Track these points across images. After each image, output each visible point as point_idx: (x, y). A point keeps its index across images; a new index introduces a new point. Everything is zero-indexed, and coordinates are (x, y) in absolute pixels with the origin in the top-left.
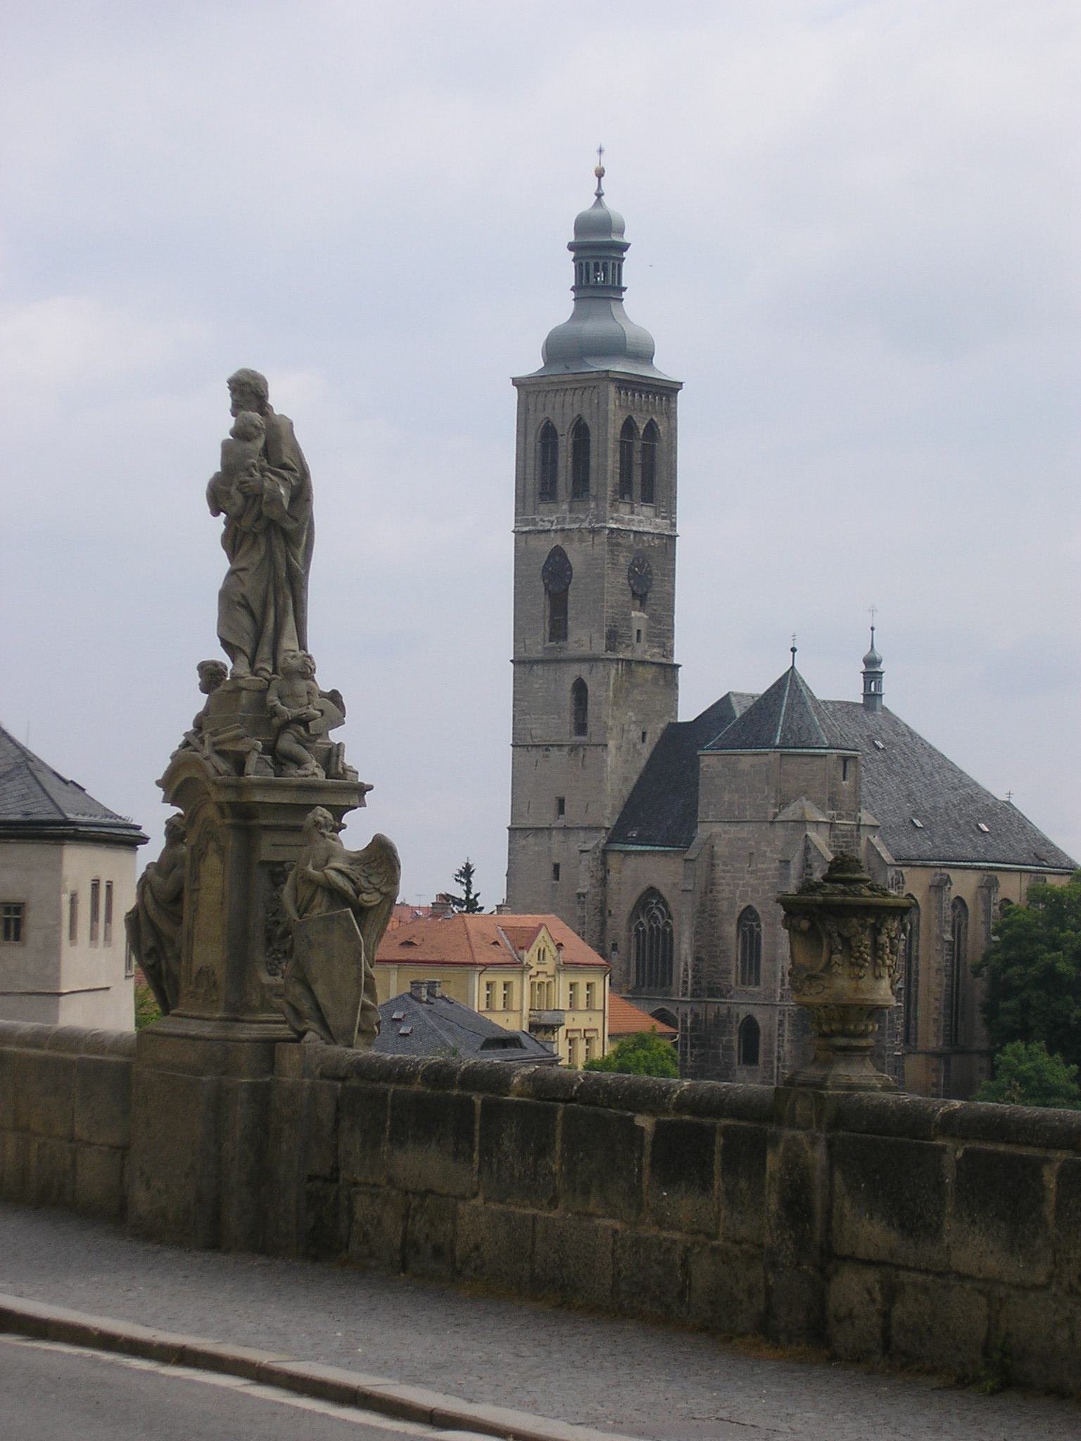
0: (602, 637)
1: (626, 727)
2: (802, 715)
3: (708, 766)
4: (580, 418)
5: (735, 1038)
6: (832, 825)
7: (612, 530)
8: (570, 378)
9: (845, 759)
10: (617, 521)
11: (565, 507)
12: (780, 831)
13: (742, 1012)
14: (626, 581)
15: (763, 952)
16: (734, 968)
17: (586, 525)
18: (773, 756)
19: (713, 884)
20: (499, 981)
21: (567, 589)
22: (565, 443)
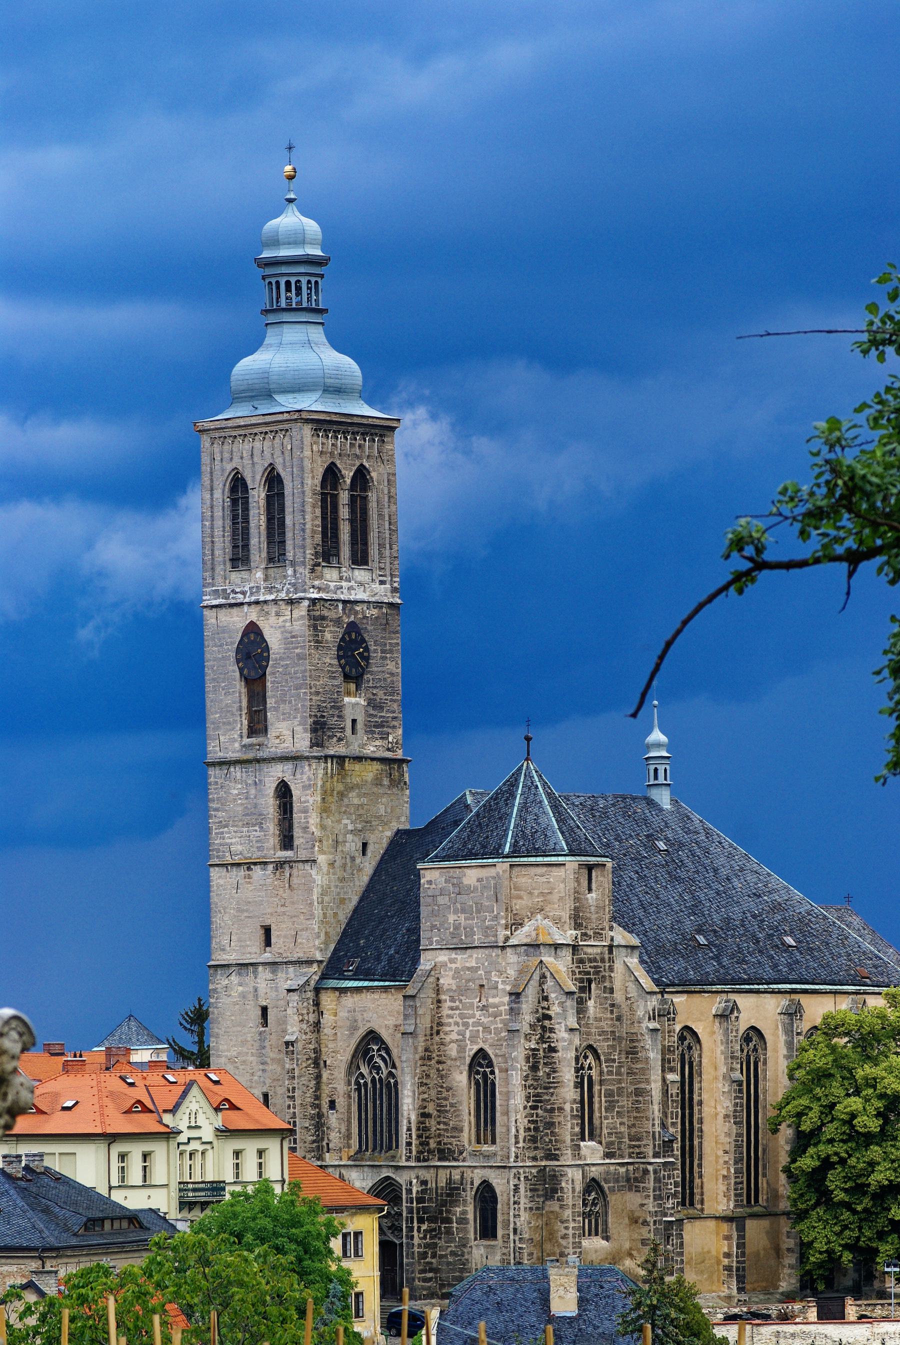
0: (305, 730)
1: (340, 839)
3: (430, 882)
4: (272, 467)
5: (470, 1209)
6: (575, 948)
7: (314, 601)
8: (261, 420)
9: (590, 868)
10: (320, 589)
11: (259, 575)
12: (511, 956)
13: (478, 1177)
14: (335, 662)
15: (498, 1103)
16: (466, 1124)
17: (283, 595)
18: (502, 866)
19: (440, 1024)
20: (136, 1150)
21: (265, 673)
22: (258, 496)
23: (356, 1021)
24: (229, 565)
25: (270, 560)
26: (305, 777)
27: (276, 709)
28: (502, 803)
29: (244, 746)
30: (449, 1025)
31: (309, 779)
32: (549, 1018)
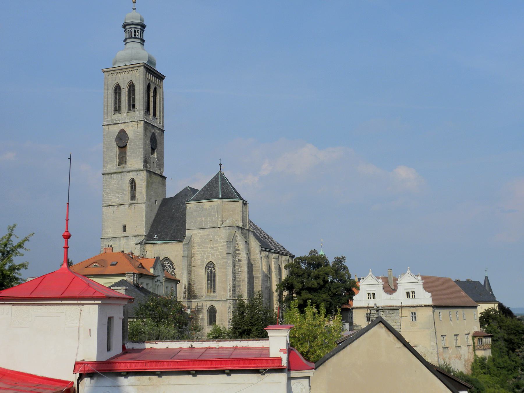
2: (227, 188)
3: (190, 208)
7: (145, 122)
10: (147, 119)
11: (125, 114)
17: (135, 120)
18: (219, 201)
24: (113, 113)
25: (129, 110)
26: (141, 177)
27: (131, 156)
28: (214, 183)
29: (118, 168)
30: (198, 254)
31: (143, 177)
32: (239, 250)
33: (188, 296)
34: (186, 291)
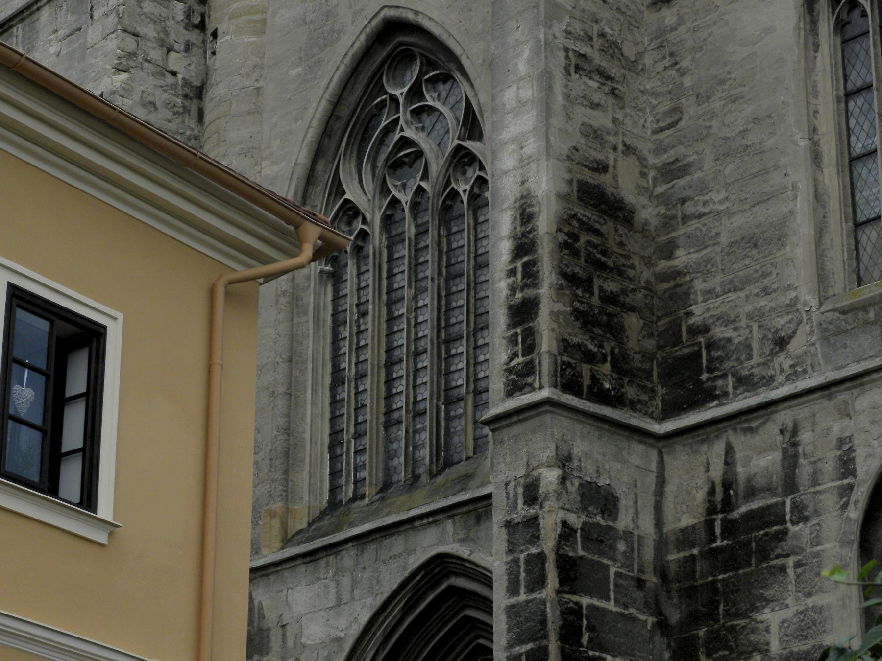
16: (802, 204)
23: (329, 15)
33: (565, 345)
34: (530, 274)
